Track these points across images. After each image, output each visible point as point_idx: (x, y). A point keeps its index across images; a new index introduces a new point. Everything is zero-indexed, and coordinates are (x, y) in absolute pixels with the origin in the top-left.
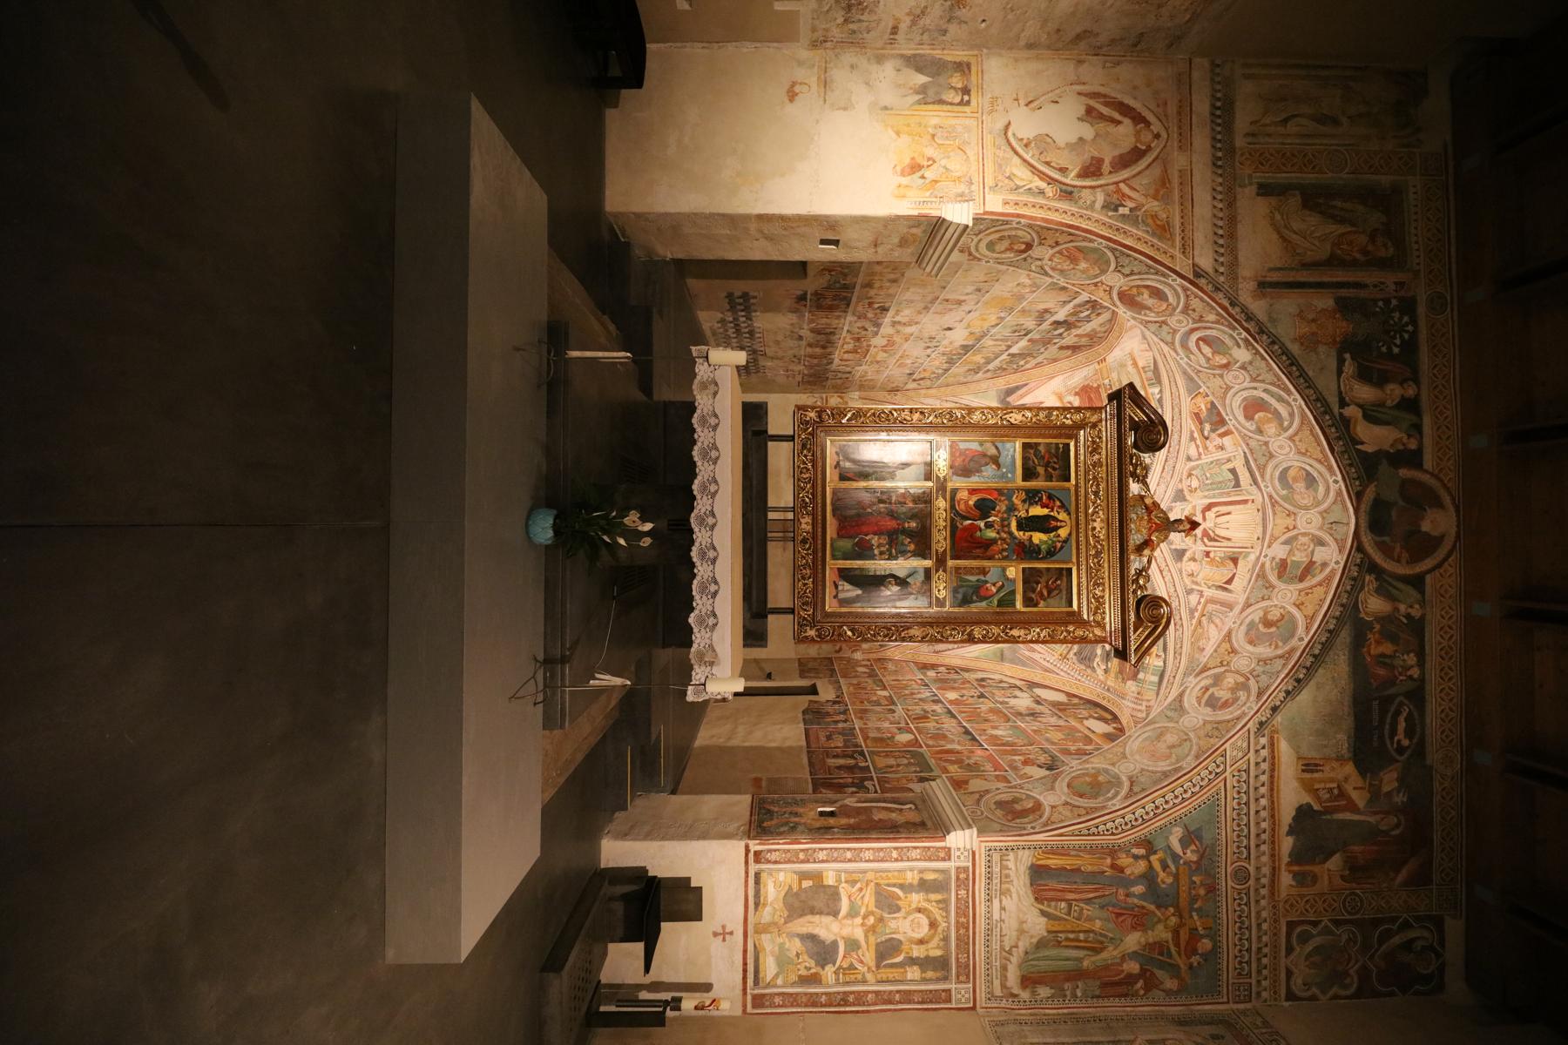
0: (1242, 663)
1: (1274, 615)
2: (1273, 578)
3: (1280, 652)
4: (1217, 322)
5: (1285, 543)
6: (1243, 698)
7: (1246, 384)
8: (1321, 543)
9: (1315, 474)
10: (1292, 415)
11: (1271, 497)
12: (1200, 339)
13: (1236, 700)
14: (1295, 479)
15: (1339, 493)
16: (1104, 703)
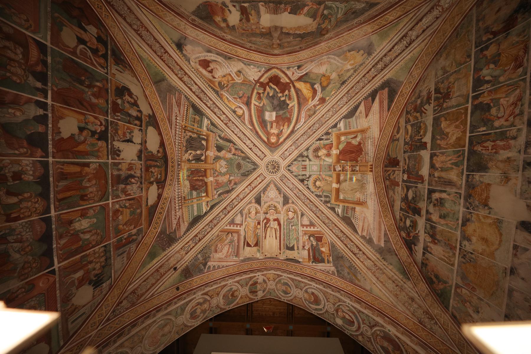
0: (214, 302)
1: (236, 294)
2: (250, 283)
3: (223, 307)
4: (357, 336)
5: (264, 280)
6: (200, 317)
7: (326, 307)
8: (264, 292)
9: (287, 295)
10: (310, 307)
11: (281, 276)
12: (353, 322)
13: (199, 316)
14: (286, 288)
15: (280, 298)
16: (170, 164)
